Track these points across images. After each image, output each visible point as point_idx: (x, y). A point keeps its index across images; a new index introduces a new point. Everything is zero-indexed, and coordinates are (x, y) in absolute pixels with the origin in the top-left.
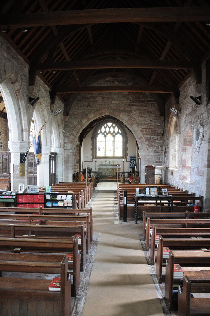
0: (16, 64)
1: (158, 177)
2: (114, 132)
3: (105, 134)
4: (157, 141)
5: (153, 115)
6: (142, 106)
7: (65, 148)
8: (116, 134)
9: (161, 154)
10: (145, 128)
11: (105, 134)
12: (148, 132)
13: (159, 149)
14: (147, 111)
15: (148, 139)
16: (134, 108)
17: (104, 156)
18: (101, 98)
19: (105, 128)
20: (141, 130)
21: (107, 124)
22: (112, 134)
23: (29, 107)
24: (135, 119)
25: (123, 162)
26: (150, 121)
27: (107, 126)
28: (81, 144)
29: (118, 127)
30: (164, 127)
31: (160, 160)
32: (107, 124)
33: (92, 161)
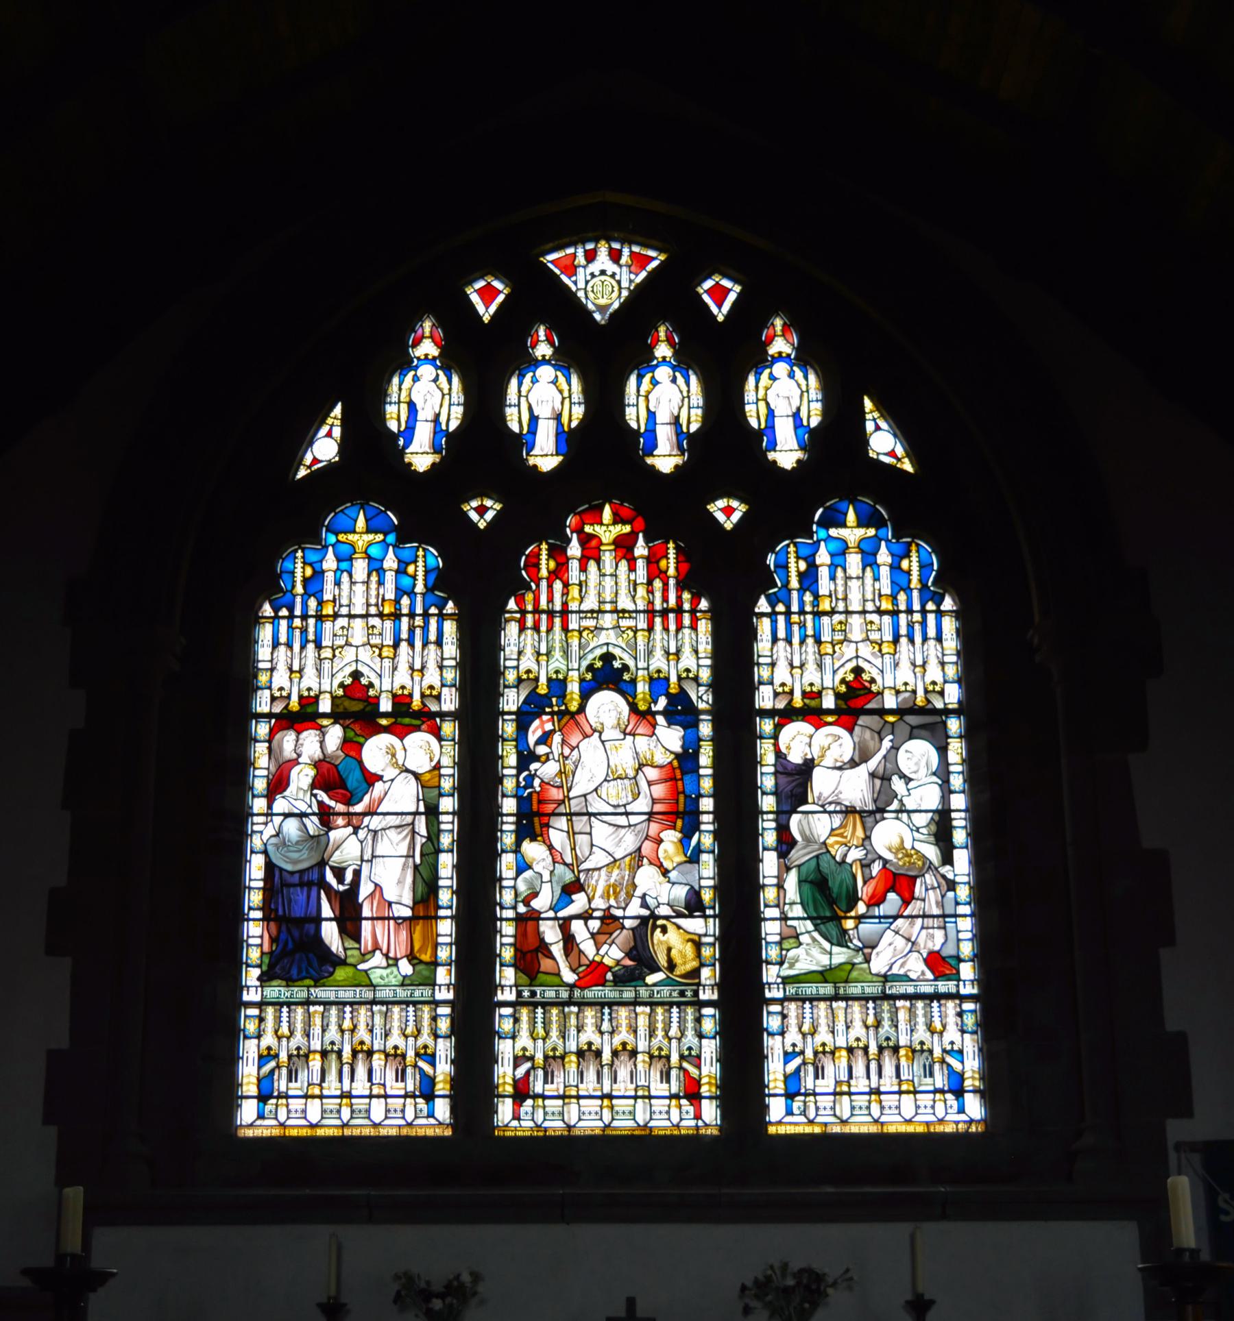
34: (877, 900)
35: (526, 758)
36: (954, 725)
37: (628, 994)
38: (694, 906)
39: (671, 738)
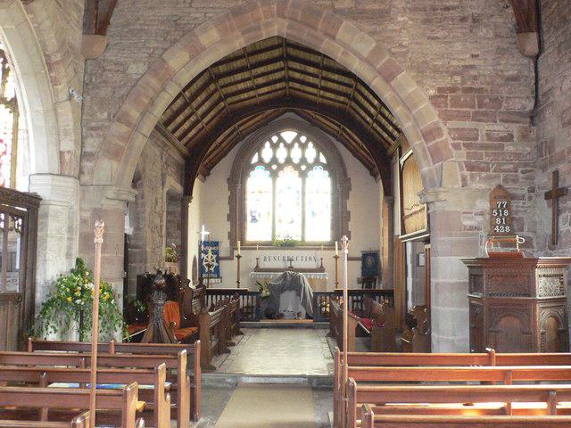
1: (547, 312)
2: (303, 160)
3: (274, 168)
4: (509, 148)
5: (482, 32)
7: (85, 178)
8: (310, 167)
10: (453, 90)
11: (274, 167)
13: (515, 181)
14: (455, 14)
17: (270, 239)
19: (275, 146)
20: (431, 98)
21: (283, 135)
22: (297, 167)
25: (336, 257)
27: (281, 140)
28: (188, 192)
29: (316, 146)
30: (536, 84)
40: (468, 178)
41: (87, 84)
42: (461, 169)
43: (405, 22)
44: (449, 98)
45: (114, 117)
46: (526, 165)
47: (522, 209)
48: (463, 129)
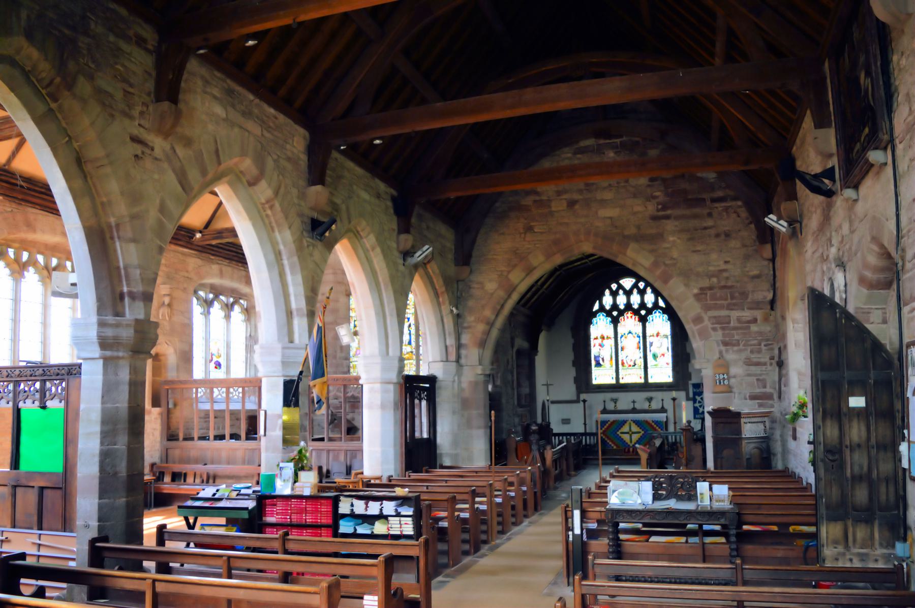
0: (257, 130)
2: (643, 305)
4: (754, 328)
5: (734, 243)
6: (696, 216)
8: (649, 312)
9: (769, 368)
10: (711, 288)
11: (615, 313)
12: (721, 298)
13: (759, 351)
14: (713, 232)
15: (723, 323)
16: (670, 225)
17: (614, 382)
18: (565, 204)
19: (614, 294)
21: (621, 282)
22: (636, 312)
23: (311, 248)
24: (674, 259)
25: (674, 399)
26: (726, 262)
27: (620, 287)
31: (768, 390)
32: (621, 282)
33: (577, 401)
34: (660, 357)
35: (621, 342)
36: (670, 337)
37: (634, 367)
38: (640, 358)
39: (638, 338)
40: (724, 352)
41: (459, 298)
42: (718, 345)
43: (674, 241)
44: (708, 295)
45: (478, 319)
46: (768, 340)
47: (764, 372)
48: (720, 317)
